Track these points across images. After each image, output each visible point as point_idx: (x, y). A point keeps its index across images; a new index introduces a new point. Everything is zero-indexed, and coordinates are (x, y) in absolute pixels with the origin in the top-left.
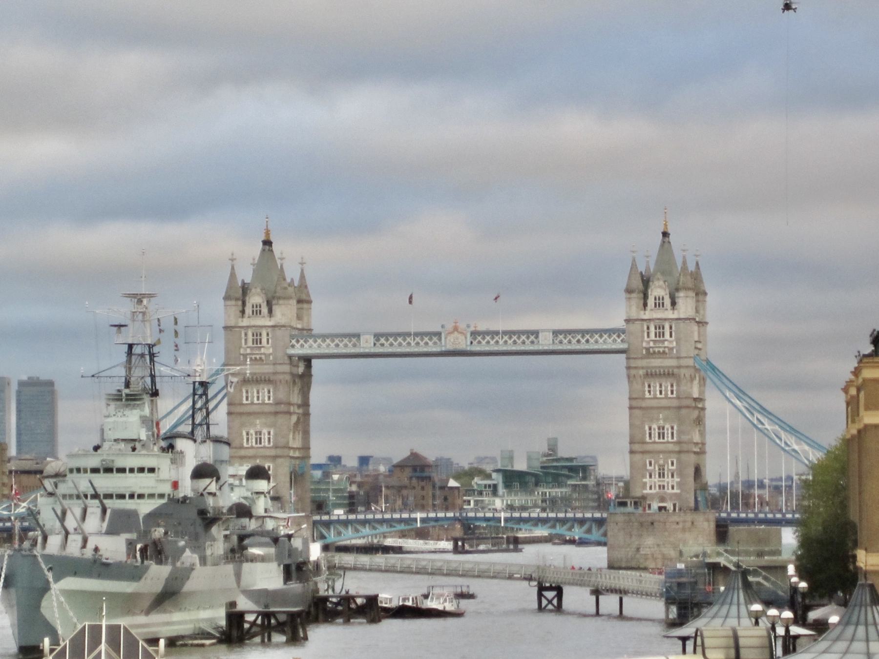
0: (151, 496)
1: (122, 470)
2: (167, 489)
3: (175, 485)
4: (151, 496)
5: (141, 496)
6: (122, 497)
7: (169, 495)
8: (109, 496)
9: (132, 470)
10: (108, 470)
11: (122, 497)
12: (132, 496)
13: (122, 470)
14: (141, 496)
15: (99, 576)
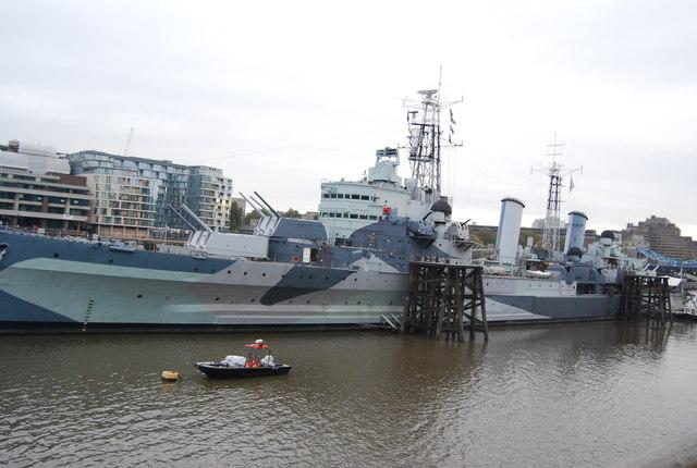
0: (363, 217)
1: (341, 196)
2: (379, 213)
3: (387, 211)
4: (363, 217)
5: (354, 216)
6: (339, 215)
7: (381, 218)
8: (332, 215)
9: (347, 196)
10: (334, 196)
11: (339, 215)
12: (346, 216)
13: (341, 196)
14: (354, 216)
15: (111, 262)
